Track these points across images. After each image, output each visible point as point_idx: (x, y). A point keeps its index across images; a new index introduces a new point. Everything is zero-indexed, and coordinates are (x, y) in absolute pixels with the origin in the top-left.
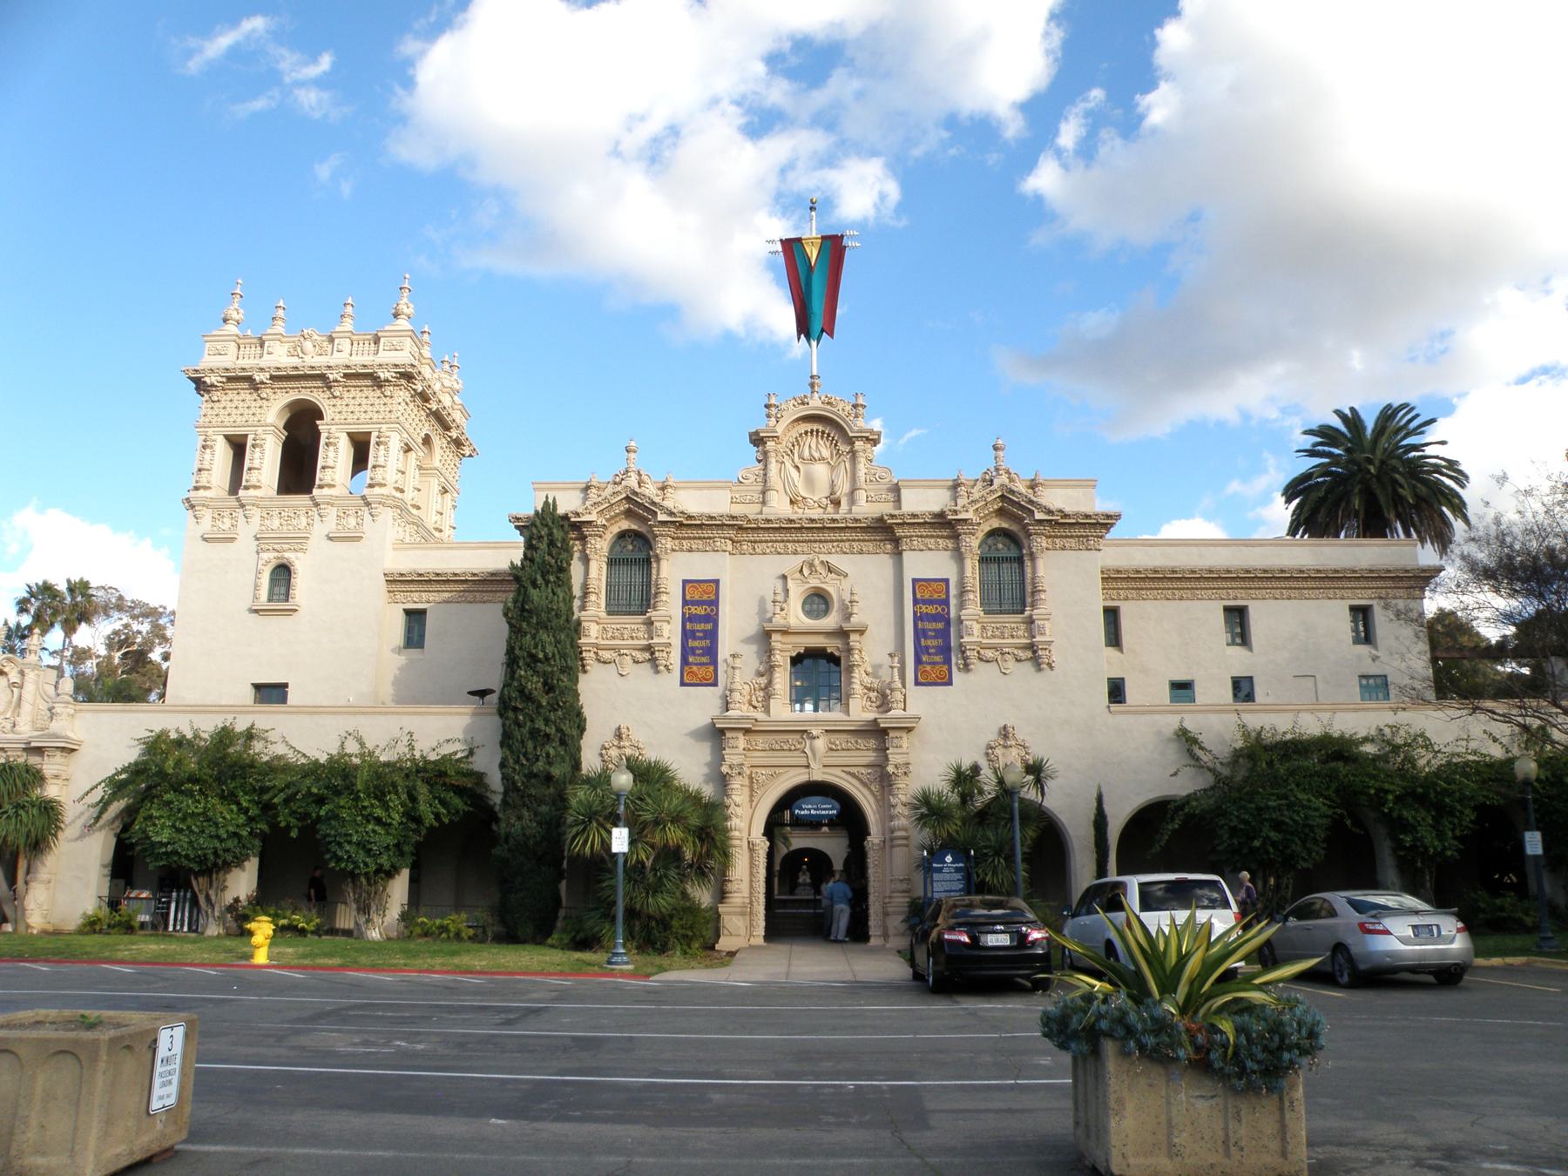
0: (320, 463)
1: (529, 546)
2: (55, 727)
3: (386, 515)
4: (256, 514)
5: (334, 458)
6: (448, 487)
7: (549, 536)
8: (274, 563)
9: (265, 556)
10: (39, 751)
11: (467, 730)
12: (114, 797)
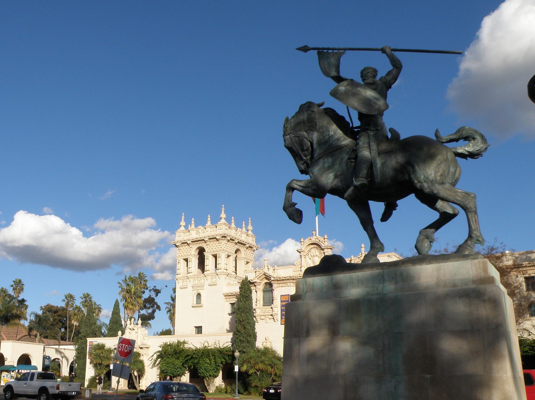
0: (206, 264)
1: (241, 291)
2: (145, 342)
3: (223, 277)
4: (192, 280)
5: (209, 262)
6: (248, 261)
7: (246, 286)
8: (196, 295)
9: (194, 292)
10: (141, 348)
11: (232, 339)
12: (157, 358)
